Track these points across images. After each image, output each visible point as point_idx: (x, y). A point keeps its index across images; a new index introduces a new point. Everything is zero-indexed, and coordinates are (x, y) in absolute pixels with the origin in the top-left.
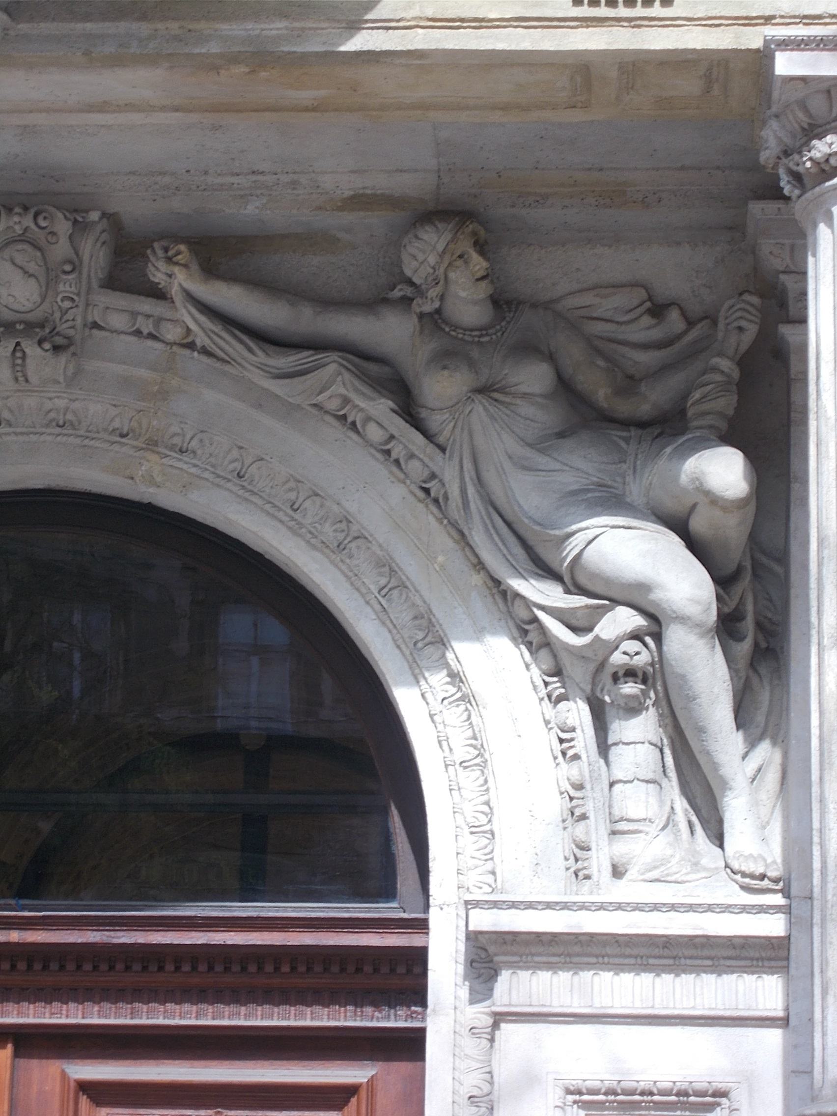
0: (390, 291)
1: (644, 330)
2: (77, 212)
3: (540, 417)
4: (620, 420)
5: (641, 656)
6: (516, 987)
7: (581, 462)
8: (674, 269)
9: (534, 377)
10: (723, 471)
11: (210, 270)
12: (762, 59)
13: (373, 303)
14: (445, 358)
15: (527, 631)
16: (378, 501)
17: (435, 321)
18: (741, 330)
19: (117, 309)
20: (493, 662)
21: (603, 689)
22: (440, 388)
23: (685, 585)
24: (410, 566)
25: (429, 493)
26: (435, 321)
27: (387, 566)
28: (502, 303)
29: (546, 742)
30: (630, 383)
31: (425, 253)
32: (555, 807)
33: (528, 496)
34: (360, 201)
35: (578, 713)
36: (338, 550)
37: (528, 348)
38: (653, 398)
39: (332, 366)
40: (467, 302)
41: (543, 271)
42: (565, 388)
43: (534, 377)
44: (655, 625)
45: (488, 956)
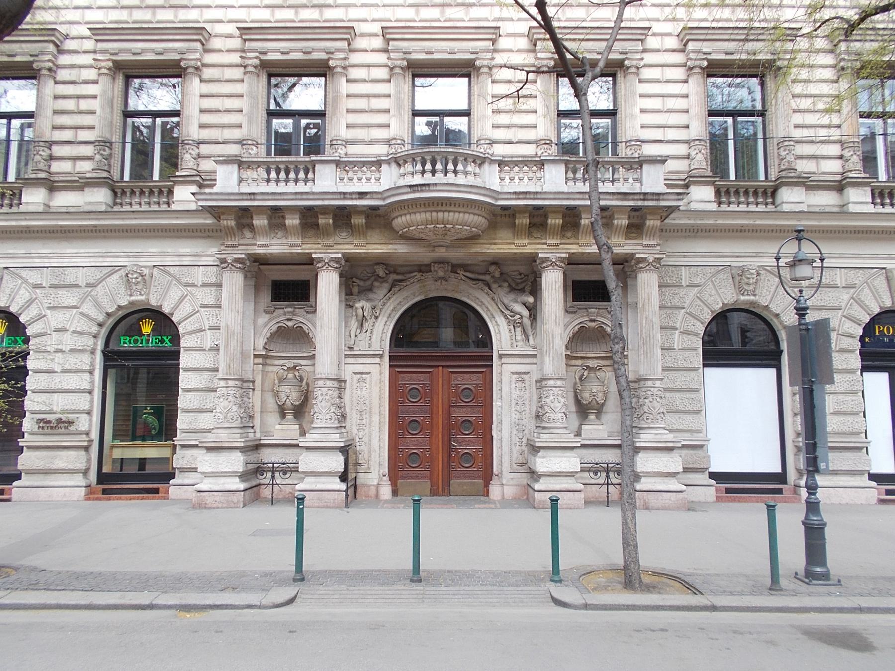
0: (487, 272)
1: (519, 277)
2: (448, 263)
3: (507, 290)
4: (516, 288)
5: (519, 320)
6: (504, 360)
7: (512, 296)
8: (522, 269)
9: (506, 284)
10: (531, 300)
11: (465, 271)
12: (537, 254)
13: (484, 274)
14: (495, 282)
15: (505, 316)
16: (486, 300)
17: (493, 277)
18: (531, 278)
19: (453, 275)
20: (501, 320)
21: (516, 324)
22: (494, 286)
23: (526, 313)
24: (490, 308)
25: (493, 299)
26: (493, 277)
27: (492, 314)
28: (502, 274)
29: (507, 330)
30: (517, 284)
31: (492, 269)
32: (509, 338)
33: (506, 301)
34: (484, 261)
35: (512, 327)
36: (480, 306)
37: (505, 281)
38: (520, 287)
39: (480, 283)
40: (497, 275)
41: (506, 269)
42: (510, 285)
43: (506, 284)
44: (522, 317)
45: (501, 356)
